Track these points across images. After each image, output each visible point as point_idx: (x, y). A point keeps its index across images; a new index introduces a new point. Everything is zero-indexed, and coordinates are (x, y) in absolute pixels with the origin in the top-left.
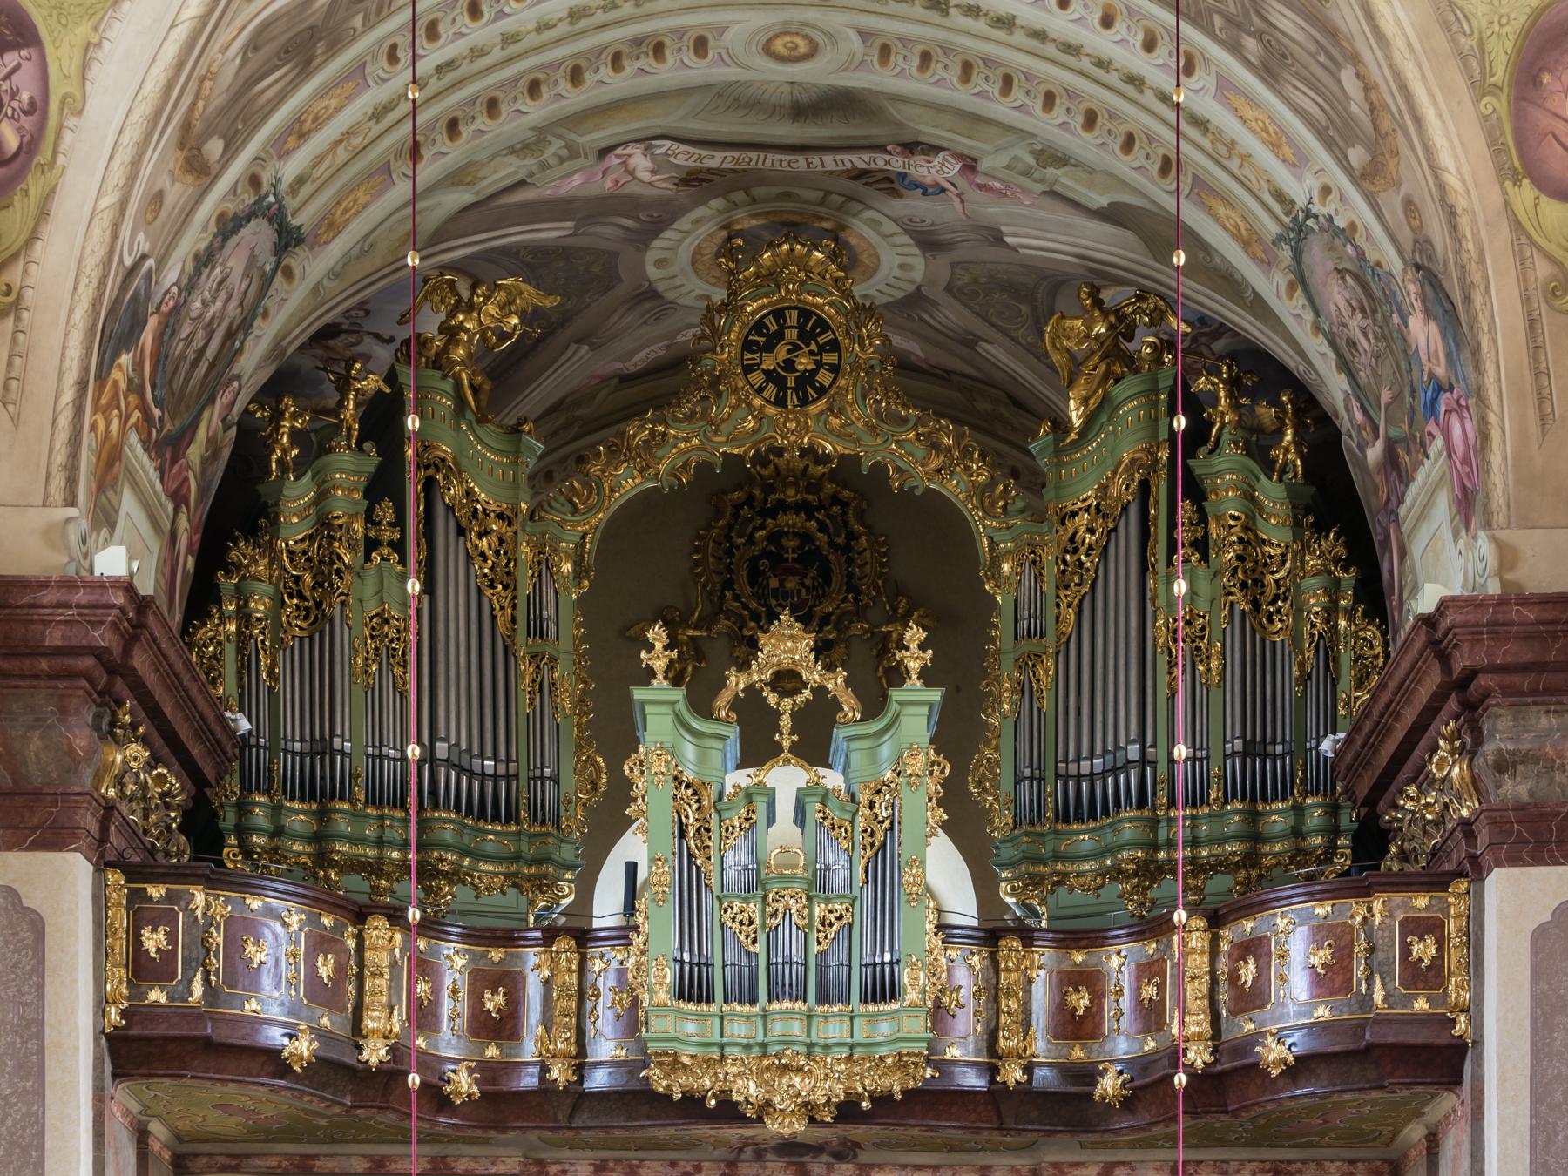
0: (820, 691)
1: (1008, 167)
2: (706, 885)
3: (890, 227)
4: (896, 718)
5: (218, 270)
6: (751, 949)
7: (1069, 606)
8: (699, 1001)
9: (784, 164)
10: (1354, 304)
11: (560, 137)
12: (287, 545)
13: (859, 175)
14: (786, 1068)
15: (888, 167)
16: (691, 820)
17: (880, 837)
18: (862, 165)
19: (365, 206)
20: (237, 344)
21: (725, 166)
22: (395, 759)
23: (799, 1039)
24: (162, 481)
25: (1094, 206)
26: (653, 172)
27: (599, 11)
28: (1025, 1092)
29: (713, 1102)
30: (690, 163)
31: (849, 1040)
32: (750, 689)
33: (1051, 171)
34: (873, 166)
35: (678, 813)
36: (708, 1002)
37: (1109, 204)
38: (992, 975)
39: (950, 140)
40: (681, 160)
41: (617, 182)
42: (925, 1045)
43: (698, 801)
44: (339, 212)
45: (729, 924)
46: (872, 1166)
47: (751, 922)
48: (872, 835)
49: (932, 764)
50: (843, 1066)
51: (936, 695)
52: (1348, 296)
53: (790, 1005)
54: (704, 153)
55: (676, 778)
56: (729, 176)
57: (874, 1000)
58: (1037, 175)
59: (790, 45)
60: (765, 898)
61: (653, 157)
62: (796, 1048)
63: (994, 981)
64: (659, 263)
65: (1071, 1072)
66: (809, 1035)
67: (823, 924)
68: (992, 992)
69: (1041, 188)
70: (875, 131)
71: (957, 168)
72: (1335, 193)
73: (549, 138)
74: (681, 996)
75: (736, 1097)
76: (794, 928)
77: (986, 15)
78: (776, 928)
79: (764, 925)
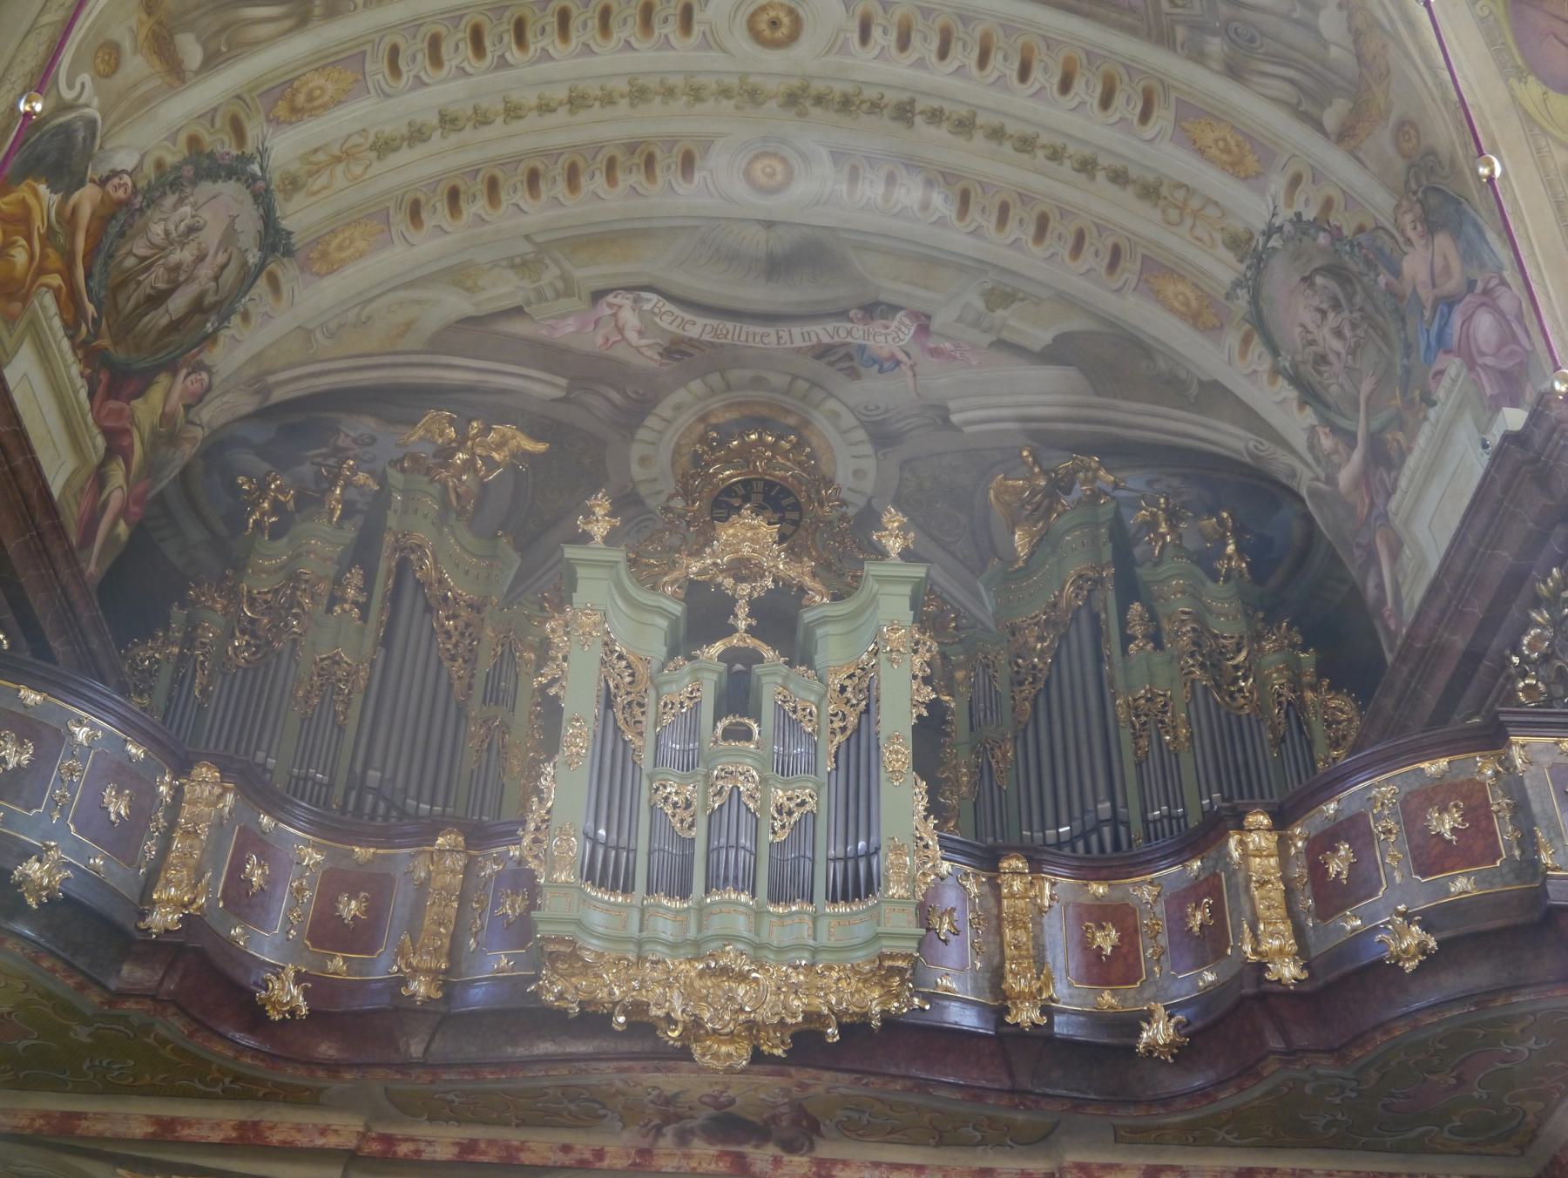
1: (959, 319)
2: (634, 763)
3: (848, 420)
4: (873, 599)
5: (186, 209)
6: (686, 835)
7: (1025, 699)
8: (613, 889)
9: (758, 338)
10: (1324, 306)
11: (556, 262)
12: (249, 592)
13: (823, 352)
14: (725, 971)
15: (849, 340)
16: (623, 692)
17: (852, 720)
18: (826, 340)
19: (362, 255)
20: (209, 327)
21: (706, 337)
22: (321, 785)
23: (745, 934)
24: (91, 395)
25: (1037, 348)
26: (641, 333)
27: (597, 104)
28: (1041, 1037)
29: (622, 1019)
30: (673, 328)
31: (811, 942)
33: (1000, 313)
34: (836, 339)
35: (606, 681)
36: (625, 891)
37: (1055, 339)
38: (991, 902)
41: (608, 340)
42: (915, 944)
43: (632, 675)
44: (334, 244)
46: (834, 1162)
47: (688, 804)
48: (844, 717)
49: (917, 643)
50: (802, 977)
51: (919, 571)
52: (1316, 302)
53: (733, 896)
54: (687, 317)
55: (606, 644)
57: (845, 898)
59: (768, 170)
60: (707, 776)
61: (641, 314)
62: (741, 946)
64: (644, 461)
65: (1098, 1019)
66: (757, 934)
67: (780, 812)
68: (994, 922)
69: (989, 338)
71: (912, 332)
72: (1307, 177)
73: (547, 261)
74: (590, 877)
76: (743, 809)
77: (948, 119)
78: (721, 807)
79: (705, 805)
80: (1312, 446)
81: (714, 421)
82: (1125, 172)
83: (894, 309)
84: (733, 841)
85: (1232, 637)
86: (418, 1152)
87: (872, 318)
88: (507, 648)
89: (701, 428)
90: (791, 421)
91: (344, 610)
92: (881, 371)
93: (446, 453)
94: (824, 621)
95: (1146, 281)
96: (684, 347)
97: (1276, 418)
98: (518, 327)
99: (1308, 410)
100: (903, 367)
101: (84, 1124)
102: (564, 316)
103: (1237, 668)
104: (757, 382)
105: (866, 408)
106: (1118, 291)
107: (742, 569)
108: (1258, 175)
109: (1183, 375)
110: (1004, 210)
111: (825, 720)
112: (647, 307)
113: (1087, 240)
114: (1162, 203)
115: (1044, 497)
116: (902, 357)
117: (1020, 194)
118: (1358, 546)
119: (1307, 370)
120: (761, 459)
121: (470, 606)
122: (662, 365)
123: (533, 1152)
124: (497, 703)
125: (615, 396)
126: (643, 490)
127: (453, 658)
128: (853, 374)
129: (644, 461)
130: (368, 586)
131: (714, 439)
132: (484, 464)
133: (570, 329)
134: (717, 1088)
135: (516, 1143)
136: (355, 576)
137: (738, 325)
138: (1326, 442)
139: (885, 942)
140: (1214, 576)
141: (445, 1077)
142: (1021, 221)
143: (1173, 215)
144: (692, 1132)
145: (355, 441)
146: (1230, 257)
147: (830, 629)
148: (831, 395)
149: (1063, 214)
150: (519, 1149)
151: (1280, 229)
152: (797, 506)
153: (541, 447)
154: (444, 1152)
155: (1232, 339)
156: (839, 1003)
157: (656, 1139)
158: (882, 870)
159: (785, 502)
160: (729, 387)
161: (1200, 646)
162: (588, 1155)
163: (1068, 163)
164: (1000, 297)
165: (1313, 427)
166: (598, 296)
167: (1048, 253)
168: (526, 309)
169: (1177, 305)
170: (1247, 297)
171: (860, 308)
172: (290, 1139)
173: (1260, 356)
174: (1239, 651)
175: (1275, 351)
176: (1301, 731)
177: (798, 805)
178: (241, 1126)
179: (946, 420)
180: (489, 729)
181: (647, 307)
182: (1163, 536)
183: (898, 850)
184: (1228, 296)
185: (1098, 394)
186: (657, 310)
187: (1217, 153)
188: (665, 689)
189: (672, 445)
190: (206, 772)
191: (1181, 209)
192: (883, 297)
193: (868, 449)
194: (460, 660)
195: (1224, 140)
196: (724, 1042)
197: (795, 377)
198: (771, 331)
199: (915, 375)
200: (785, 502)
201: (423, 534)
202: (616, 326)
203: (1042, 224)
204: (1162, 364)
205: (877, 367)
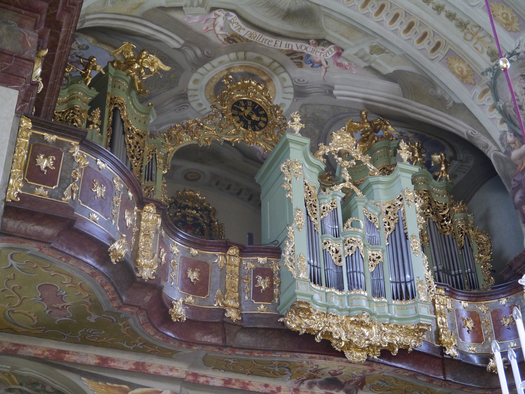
0: (359, 162)
1: (356, 54)
2: (315, 231)
4: (398, 176)
6: (338, 264)
9: (267, 42)
13: (291, 54)
15: (305, 51)
18: (295, 49)
21: (246, 37)
25: (385, 72)
26: (222, 29)
30: (235, 30)
32: (330, 153)
33: (375, 56)
34: (300, 50)
37: (394, 72)
39: (339, 40)
40: (233, 27)
41: (208, 28)
45: (328, 250)
51: (416, 169)
54: (243, 26)
56: (245, 42)
58: (366, 58)
63: (433, 308)
69: (366, 64)
70: (310, 32)
71: (333, 54)
75: (335, 336)
78: (352, 255)
80: (501, 139)
81: (232, 71)
82: (455, 15)
83: (330, 43)
84: (355, 270)
85: (442, 204)
86: (207, 381)
87: (319, 45)
88: (154, 156)
89: (226, 73)
90: (264, 78)
91: (94, 128)
92: (312, 67)
93: (129, 64)
94: (378, 182)
95: (447, 59)
96: (235, 39)
97: (487, 125)
98: (177, 15)
99: (505, 125)
100: (322, 67)
101: (67, 356)
102: (196, 15)
103: (444, 216)
104: (258, 59)
105: (299, 80)
106: (432, 60)
107: (345, 155)
108: (517, 31)
109: (447, 98)
110: (396, 16)
111: (382, 224)
112: (229, 18)
113: (427, 37)
114: (466, 31)
115: (371, 133)
116: (324, 63)
117: (406, 12)
118: (514, 180)
119: (511, 111)
120: (252, 92)
121: (138, 134)
122: (224, 43)
123: (253, 386)
124: (151, 180)
125: (199, 52)
126: (190, 93)
127: (132, 157)
128: (300, 65)
129: (196, 81)
130: (102, 118)
131: (231, 79)
132: (144, 71)
133: (196, 21)
134: (340, 368)
135: (247, 382)
136: (97, 112)
137: (262, 34)
138: (510, 138)
139: (421, 319)
140: (436, 178)
141: (237, 353)
142: (401, 23)
143: (469, 36)
144: (315, 383)
145: (79, 47)
146: (488, 59)
147: (380, 186)
148: (286, 71)
149: (421, 24)
150: (248, 384)
151: (518, 54)
152: (265, 115)
153: (167, 68)
154: (218, 383)
155: (478, 90)
156: (400, 340)
157: (300, 385)
158: (416, 290)
159: (261, 113)
160: (245, 59)
161: (431, 205)
162: (274, 389)
163: (431, 5)
164: (377, 50)
165: (505, 132)
166: (213, 9)
167: (408, 38)
168: (184, 8)
169: (457, 71)
170: (491, 76)
171: (315, 40)
172: (158, 372)
173: (488, 100)
174: (445, 209)
175: (497, 99)
176: (470, 246)
177: (377, 258)
178: (137, 364)
179: (331, 92)
180: (149, 191)
181: (229, 18)
182: (417, 158)
183: (421, 282)
184: (483, 74)
185: (404, 97)
186: (232, 21)
187: (501, 19)
188: (322, 201)
189: (211, 76)
190: (150, 208)
191: (473, 35)
192: (328, 38)
193: (291, 96)
194: (135, 158)
195: (507, 14)
196: (358, 351)
197: (275, 61)
198: (274, 40)
199: (326, 71)
200: (261, 113)
201: (123, 98)
202: (214, 24)
203: (410, 26)
204: (439, 92)
205: (311, 64)
